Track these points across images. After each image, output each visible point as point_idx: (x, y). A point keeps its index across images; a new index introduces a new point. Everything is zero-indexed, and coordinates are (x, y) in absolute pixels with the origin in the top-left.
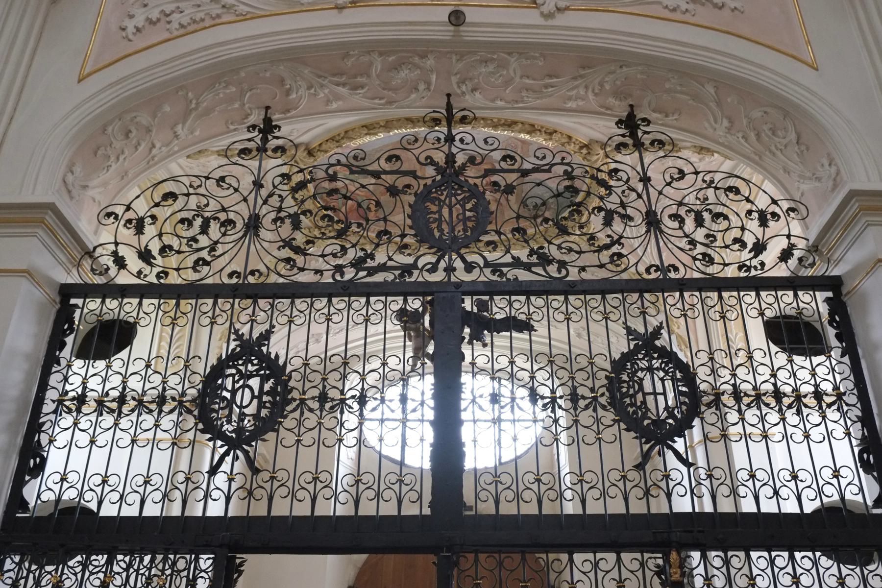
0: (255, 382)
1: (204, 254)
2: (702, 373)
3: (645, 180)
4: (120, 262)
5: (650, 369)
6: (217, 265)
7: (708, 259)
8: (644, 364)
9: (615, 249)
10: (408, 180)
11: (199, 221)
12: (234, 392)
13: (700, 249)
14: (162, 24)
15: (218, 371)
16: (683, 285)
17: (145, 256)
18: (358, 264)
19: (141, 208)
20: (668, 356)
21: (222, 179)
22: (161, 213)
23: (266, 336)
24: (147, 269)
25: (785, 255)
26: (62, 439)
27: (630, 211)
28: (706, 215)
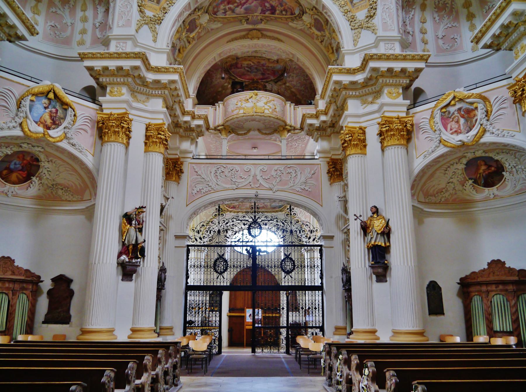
0: (222, 263)
1: (211, 238)
2: (296, 262)
3: (291, 223)
4: (196, 240)
5: (288, 261)
6: (214, 241)
7: (300, 240)
8: (287, 260)
9: (284, 238)
10: (247, 222)
11: (209, 231)
12: (219, 265)
13: (299, 238)
14: (200, 192)
15: (216, 261)
16: (295, 246)
17: (200, 238)
18: (238, 241)
19: (198, 228)
20: (291, 259)
21: (212, 222)
22: (202, 229)
23: (223, 255)
24: (201, 241)
25: (314, 240)
26: (192, 273)
27: (288, 230)
28: (301, 231)
